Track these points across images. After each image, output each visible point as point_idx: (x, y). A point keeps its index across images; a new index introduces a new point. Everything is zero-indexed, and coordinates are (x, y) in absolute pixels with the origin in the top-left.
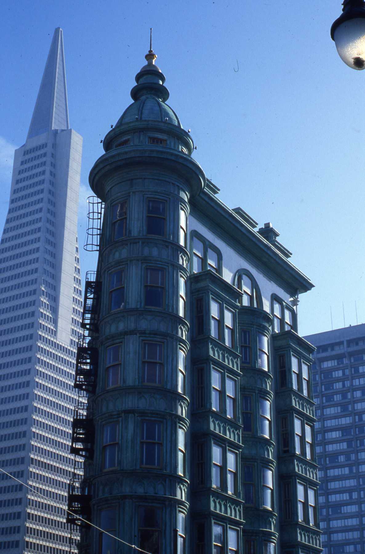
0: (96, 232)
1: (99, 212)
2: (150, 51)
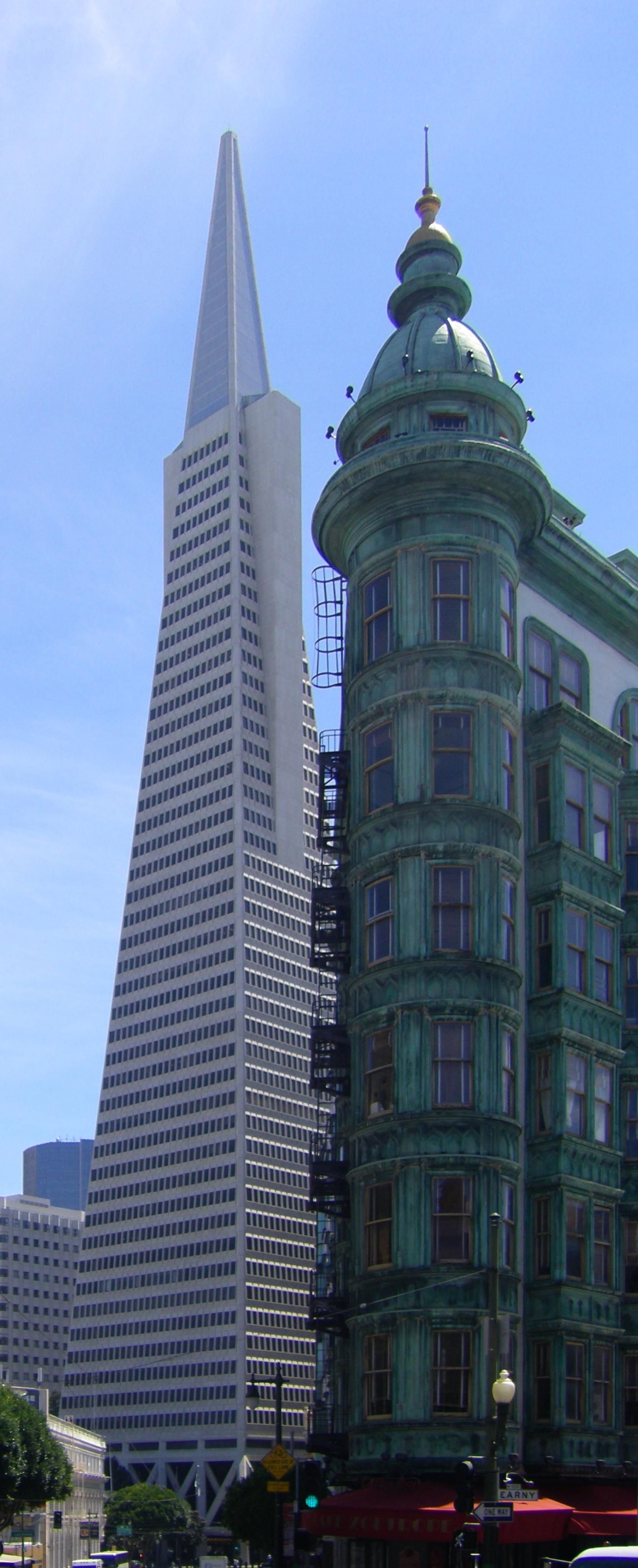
0: (333, 644)
1: (338, 599)
2: (427, 191)
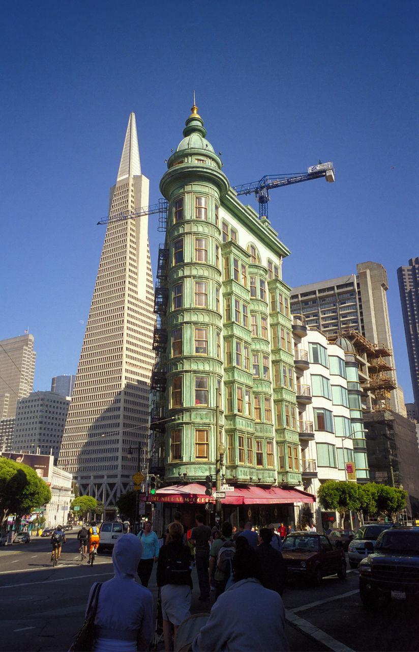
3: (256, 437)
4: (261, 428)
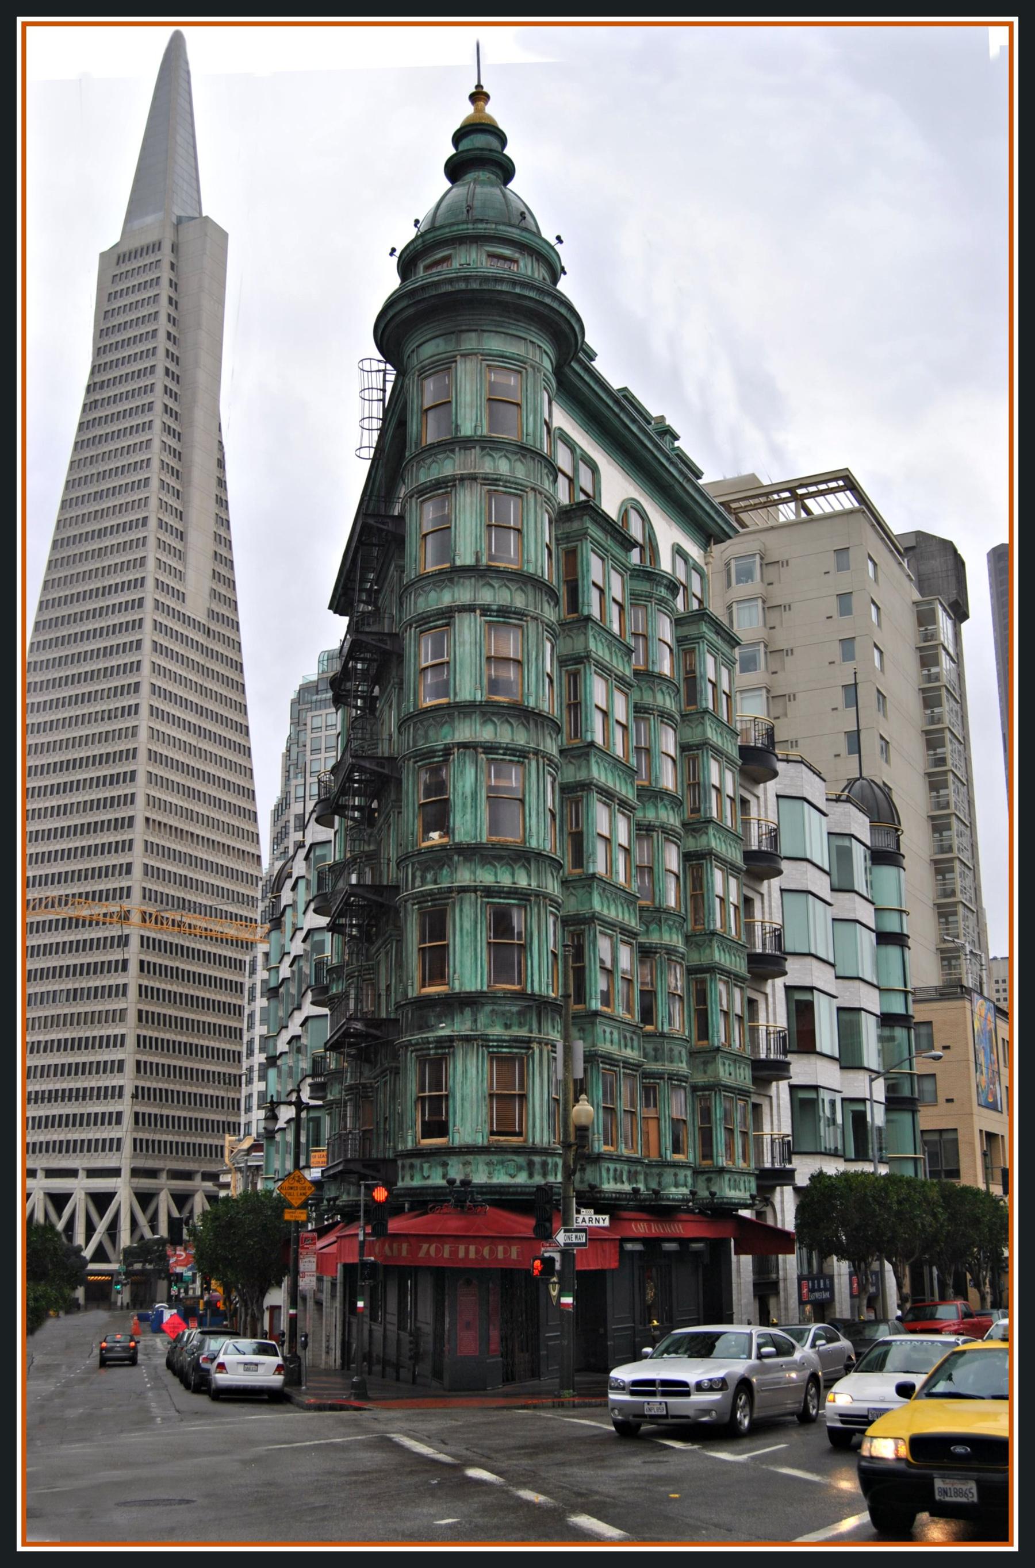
2: (479, 86)
3: (646, 1075)
4: (656, 1050)
